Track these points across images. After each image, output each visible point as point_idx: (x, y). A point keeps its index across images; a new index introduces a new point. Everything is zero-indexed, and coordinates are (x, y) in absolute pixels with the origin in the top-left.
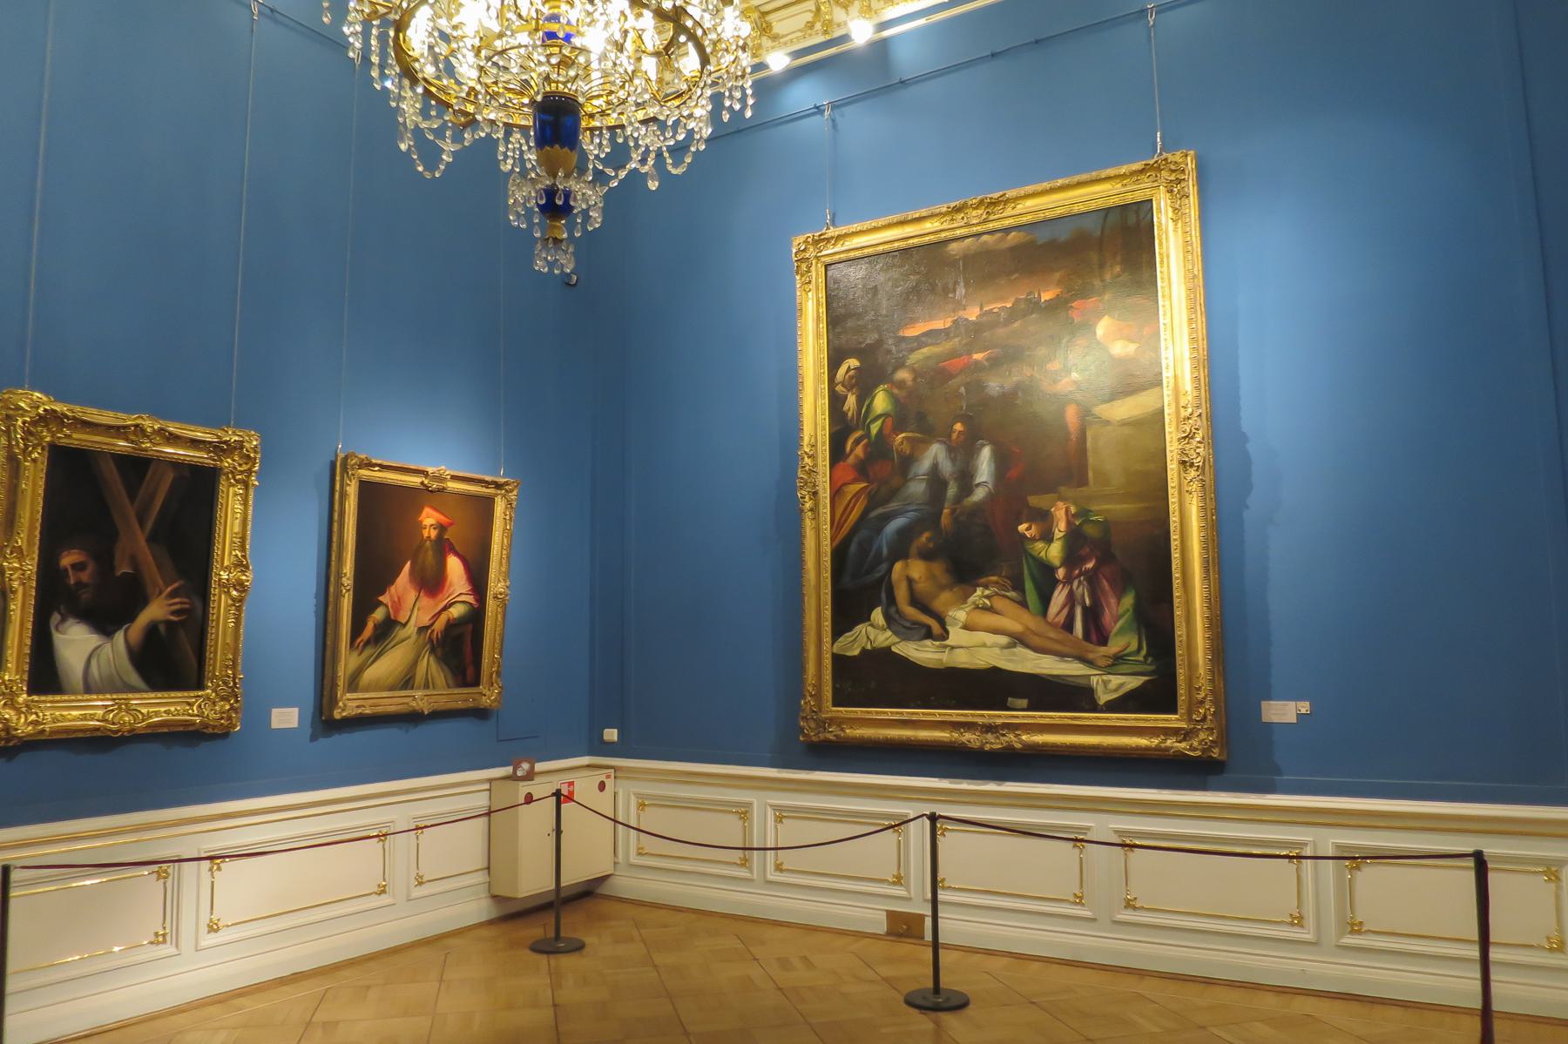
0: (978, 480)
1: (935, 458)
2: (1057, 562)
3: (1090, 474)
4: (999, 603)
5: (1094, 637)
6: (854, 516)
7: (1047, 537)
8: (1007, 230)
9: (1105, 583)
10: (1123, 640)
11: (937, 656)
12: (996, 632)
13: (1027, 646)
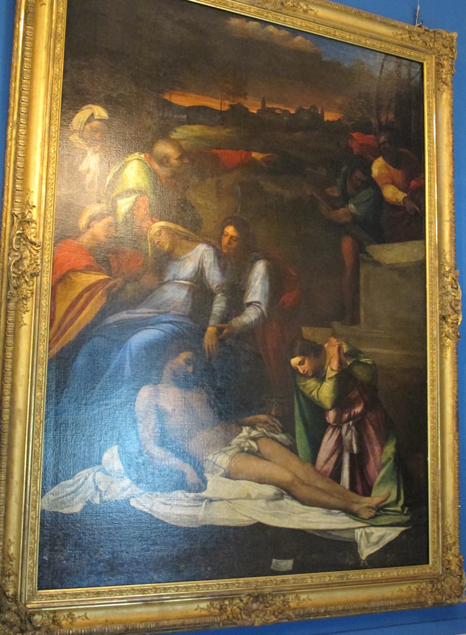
0: (250, 298)
1: (201, 262)
2: (328, 403)
3: (362, 313)
4: (268, 448)
5: (359, 488)
6: (88, 314)
7: (319, 375)
8: (295, 32)
9: (370, 427)
10: (385, 491)
11: (190, 512)
12: (261, 481)
13: (295, 498)
